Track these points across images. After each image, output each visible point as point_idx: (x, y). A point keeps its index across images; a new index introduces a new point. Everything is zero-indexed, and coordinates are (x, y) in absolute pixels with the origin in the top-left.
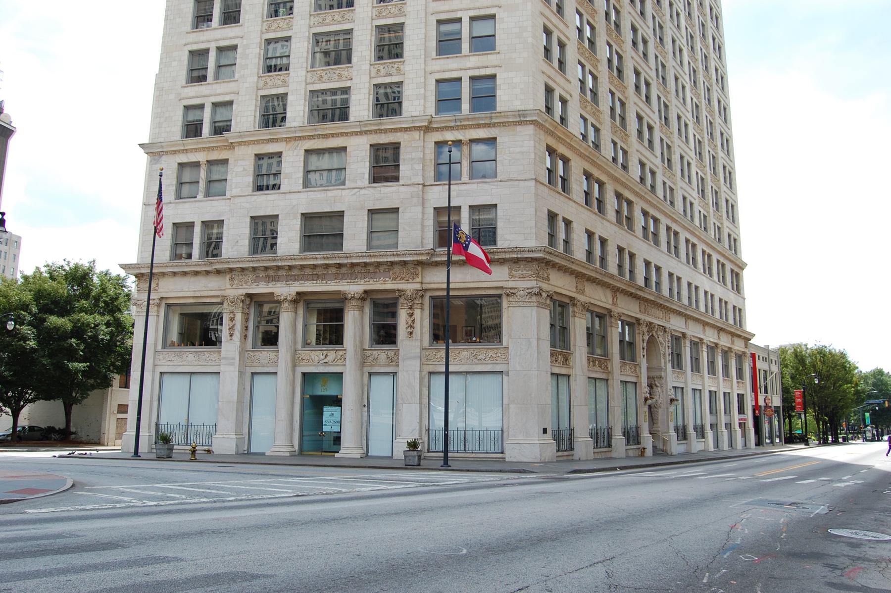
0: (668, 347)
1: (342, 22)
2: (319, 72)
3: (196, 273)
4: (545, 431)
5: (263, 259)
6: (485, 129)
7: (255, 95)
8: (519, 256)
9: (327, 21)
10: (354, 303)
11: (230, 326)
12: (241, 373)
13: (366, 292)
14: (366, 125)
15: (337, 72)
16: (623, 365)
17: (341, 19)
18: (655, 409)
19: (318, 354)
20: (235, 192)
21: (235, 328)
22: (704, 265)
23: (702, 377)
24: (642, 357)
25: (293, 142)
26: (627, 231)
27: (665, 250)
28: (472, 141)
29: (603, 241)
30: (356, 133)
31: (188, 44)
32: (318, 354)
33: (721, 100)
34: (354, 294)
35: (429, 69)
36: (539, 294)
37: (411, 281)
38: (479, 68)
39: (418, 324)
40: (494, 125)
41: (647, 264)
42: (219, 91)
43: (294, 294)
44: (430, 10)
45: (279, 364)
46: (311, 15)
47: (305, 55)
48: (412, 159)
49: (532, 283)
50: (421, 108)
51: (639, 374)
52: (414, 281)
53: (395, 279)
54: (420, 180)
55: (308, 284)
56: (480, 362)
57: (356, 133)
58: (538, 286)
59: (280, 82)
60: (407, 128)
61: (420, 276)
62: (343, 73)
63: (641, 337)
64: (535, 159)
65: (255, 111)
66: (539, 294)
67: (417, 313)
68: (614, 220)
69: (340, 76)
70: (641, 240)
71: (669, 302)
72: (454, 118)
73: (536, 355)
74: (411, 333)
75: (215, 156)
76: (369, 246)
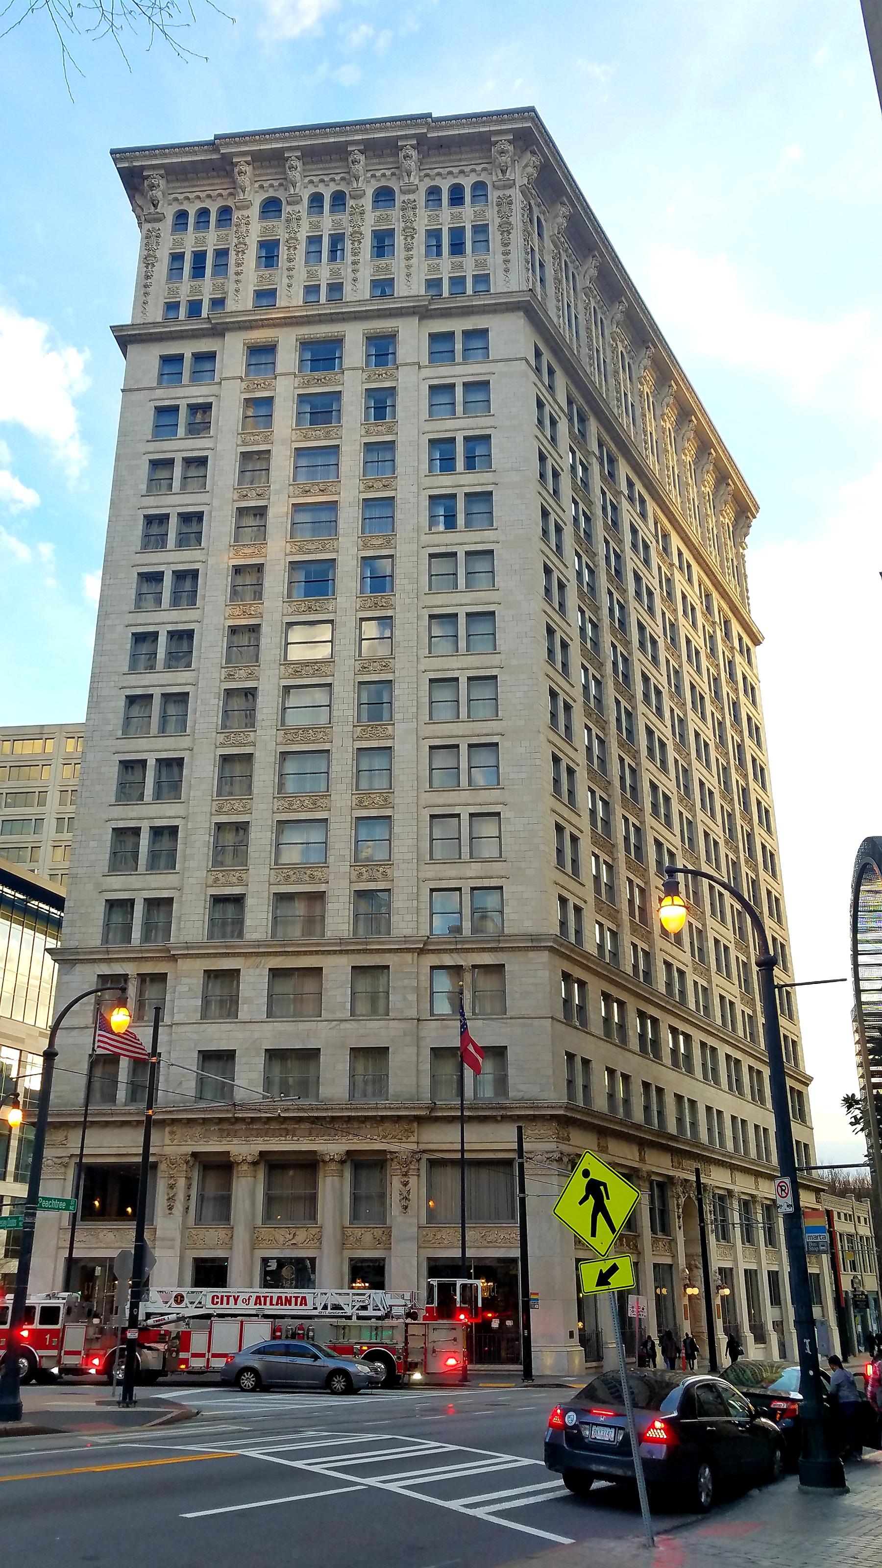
0: (710, 1211)
2: (285, 871)
3: (124, 1124)
4: (571, 1335)
5: (216, 1107)
7: (204, 895)
8: (536, 1113)
9: (295, 807)
10: (333, 1166)
12: (182, 1258)
13: (348, 1153)
14: (348, 943)
15: (308, 872)
16: (655, 1241)
17: (312, 807)
18: (696, 1301)
20: (178, 1018)
21: (175, 1198)
22: (752, 1087)
23: (757, 1251)
24: (677, 1228)
25: (254, 958)
26: (652, 1061)
27: (701, 1078)
29: (626, 1078)
30: (335, 952)
33: (766, 844)
34: (334, 1156)
35: (422, 875)
36: (560, 1160)
37: (404, 1140)
39: (413, 1196)
40: (502, 949)
41: (679, 1098)
42: (154, 885)
43: (257, 1154)
44: (422, 803)
45: (235, 1248)
46: (274, 798)
47: (268, 848)
48: (405, 987)
49: (552, 1146)
50: (414, 925)
51: (675, 1253)
52: (409, 1140)
53: (385, 1137)
54: (413, 1013)
55: (273, 1142)
56: (491, 1245)
57: (335, 952)
58: (559, 1149)
59: (234, 880)
61: (416, 1134)
62: (315, 873)
63: (676, 1202)
64: (551, 992)
65: (204, 914)
66: (560, 1160)
67: (413, 1181)
68: (637, 1048)
69: (312, 877)
70: (670, 1068)
71: (709, 1150)
72: (454, 939)
73: (558, 1237)
74: (406, 1208)
75: (148, 968)
76: (352, 1096)
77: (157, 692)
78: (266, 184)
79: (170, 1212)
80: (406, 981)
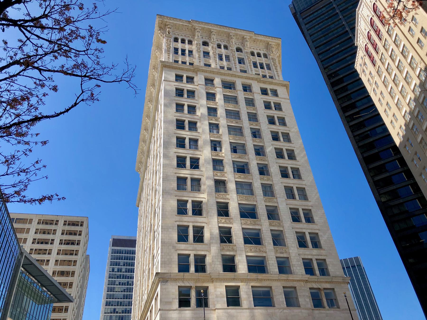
1: (255, 225)
15: (258, 248)
17: (254, 224)
28: (325, 289)
30: (276, 280)
38: (318, 255)
48: (304, 296)
60: (298, 280)
77: (189, 177)
78: (204, 37)
80: (304, 293)
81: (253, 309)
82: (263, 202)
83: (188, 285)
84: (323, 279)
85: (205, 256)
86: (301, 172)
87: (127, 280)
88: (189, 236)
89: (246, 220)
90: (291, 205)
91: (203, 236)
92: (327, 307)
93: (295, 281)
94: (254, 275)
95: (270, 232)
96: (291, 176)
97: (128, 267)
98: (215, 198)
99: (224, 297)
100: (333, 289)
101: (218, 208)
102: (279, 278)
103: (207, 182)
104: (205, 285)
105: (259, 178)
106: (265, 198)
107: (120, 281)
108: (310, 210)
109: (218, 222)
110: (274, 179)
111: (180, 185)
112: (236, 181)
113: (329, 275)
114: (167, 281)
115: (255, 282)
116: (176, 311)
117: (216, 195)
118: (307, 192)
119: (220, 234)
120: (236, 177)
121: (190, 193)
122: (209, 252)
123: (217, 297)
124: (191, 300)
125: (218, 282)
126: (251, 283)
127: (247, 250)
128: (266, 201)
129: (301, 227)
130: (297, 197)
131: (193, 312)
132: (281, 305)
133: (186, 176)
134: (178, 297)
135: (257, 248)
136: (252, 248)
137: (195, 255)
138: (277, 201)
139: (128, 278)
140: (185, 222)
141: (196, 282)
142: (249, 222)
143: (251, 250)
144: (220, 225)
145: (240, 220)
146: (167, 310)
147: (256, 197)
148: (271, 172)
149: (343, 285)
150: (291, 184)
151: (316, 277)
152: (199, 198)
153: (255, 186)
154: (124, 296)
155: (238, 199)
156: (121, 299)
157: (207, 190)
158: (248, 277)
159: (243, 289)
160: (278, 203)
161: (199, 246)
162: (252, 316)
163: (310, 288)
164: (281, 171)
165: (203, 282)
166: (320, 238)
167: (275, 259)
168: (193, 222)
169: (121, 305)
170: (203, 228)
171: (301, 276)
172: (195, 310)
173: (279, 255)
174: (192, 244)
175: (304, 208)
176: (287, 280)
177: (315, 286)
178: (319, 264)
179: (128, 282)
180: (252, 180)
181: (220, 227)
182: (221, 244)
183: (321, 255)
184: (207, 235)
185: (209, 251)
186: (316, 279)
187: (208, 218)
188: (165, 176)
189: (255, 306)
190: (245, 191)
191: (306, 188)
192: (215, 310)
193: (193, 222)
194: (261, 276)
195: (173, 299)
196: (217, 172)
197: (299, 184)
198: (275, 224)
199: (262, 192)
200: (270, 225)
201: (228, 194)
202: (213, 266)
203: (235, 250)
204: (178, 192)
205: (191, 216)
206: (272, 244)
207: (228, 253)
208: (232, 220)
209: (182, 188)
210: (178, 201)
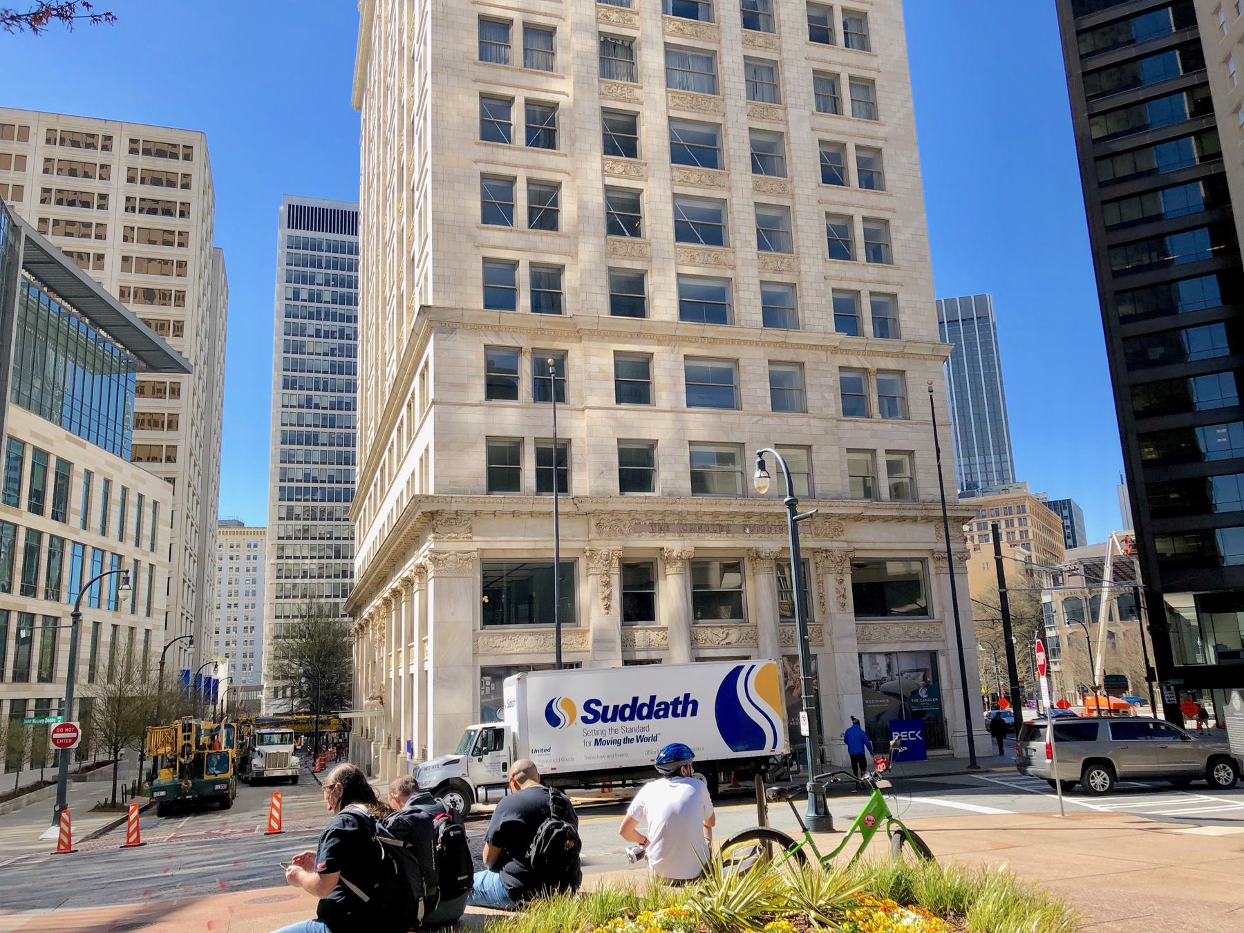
1: (712, 187)
6: (893, 359)
9: (692, 181)
11: (606, 593)
15: (712, 254)
17: (709, 183)
19: (716, 632)
28: (880, 371)
30: (751, 343)
31: (480, 161)
32: (716, 632)
37: (835, 538)
38: (879, 282)
48: (822, 386)
53: (817, 535)
57: (751, 343)
74: (843, 605)
77: (517, 18)
79: (606, 611)
80: (822, 380)
81: (684, 412)
82: (743, 118)
83: (510, 342)
84: (881, 345)
85: (560, 269)
86: (871, 26)
87: (337, 323)
88: (514, 209)
89: (688, 169)
90: (827, 131)
91: (558, 211)
92: (877, 416)
93: (804, 348)
94: (694, 328)
95: (752, 209)
96: (840, 37)
97: (339, 289)
98: (596, 95)
99: (609, 380)
100: (902, 372)
101: (605, 129)
102: (762, 337)
103: (574, 40)
104: (559, 345)
105: (740, 38)
106: (750, 104)
107: (319, 327)
108: (879, 151)
109: (603, 171)
110: (784, 46)
111: (489, 46)
112: (666, 44)
113: (897, 336)
114: (453, 330)
115: (698, 344)
116: (479, 408)
117: (603, 86)
118: (878, 94)
119: (608, 208)
120: (668, 30)
121: (519, 74)
122: (572, 257)
123: (590, 378)
124: (520, 381)
125: (596, 341)
126: (684, 347)
127: (682, 259)
128: (751, 114)
129: (843, 200)
130: (847, 107)
131: (524, 411)
132: (759, 406)
133: (510, 14)
134: (483, 374)
135: (709, 255)
136: (695, 254)
137: (532, 265)
138: (786, 115)
139: (342, 320)
140: (504, 164)
141: (533, 338)
142: (695, 178)
143: (692, 258)
144: (610, 181)
145: (669, 169)
146: (455, 404)
147: (723, 100)
148: (779, 20)
149: (928, 363)
150: (835, 63)
151: (865, 341)
152: (547, 91)
153: (725, 65)
154: (333, 365)
155: (667, 104)
156: (324, 372)
157: (574, 68)
158: (678, 333)
159: (662, 362)
160: (787, 122)
161: (543, 238)
162: (679, 430)
163: (842, 369)
164: (811, 19)
165: (554, 339)
166: (893, 235)
167: (756, 288)
168: (528, 167)
169: (325, 390)
170: (557, 186)
171: (823, 336)
172: (528, 407)
173: (768, 277)
174: (523, 232)
175: (862, 142)
176: (782, 345)
177: (856, 364)
178: (875, 308)
179: (342, 331)
180: (719, 42)
181: (608, 189)
182: (609, 237)
183: (888, 283)
184: (568, 209)
185: (574, 255)
186: (861, 344)
187: (573, 156)
188: (440, 9)
189: (689, 405)
190: (691, 78)
191: (877, 82)
192: (583, 410)
193: (528, 167)
194: (712, 330)
195: (469, 377)
196: (609, 9)
197: (858, 67)
198: (769, 187)
199: (743, 87)
200: (757, 189)
201: (639, 84)
202: (583, 296)
203: (649, 255)
204: (482, 69)
205: (521, 149)
206: (755, 244)
207: (627, 264)
208: (644, 167)
209: (494, 54)
210: (483, 96)
